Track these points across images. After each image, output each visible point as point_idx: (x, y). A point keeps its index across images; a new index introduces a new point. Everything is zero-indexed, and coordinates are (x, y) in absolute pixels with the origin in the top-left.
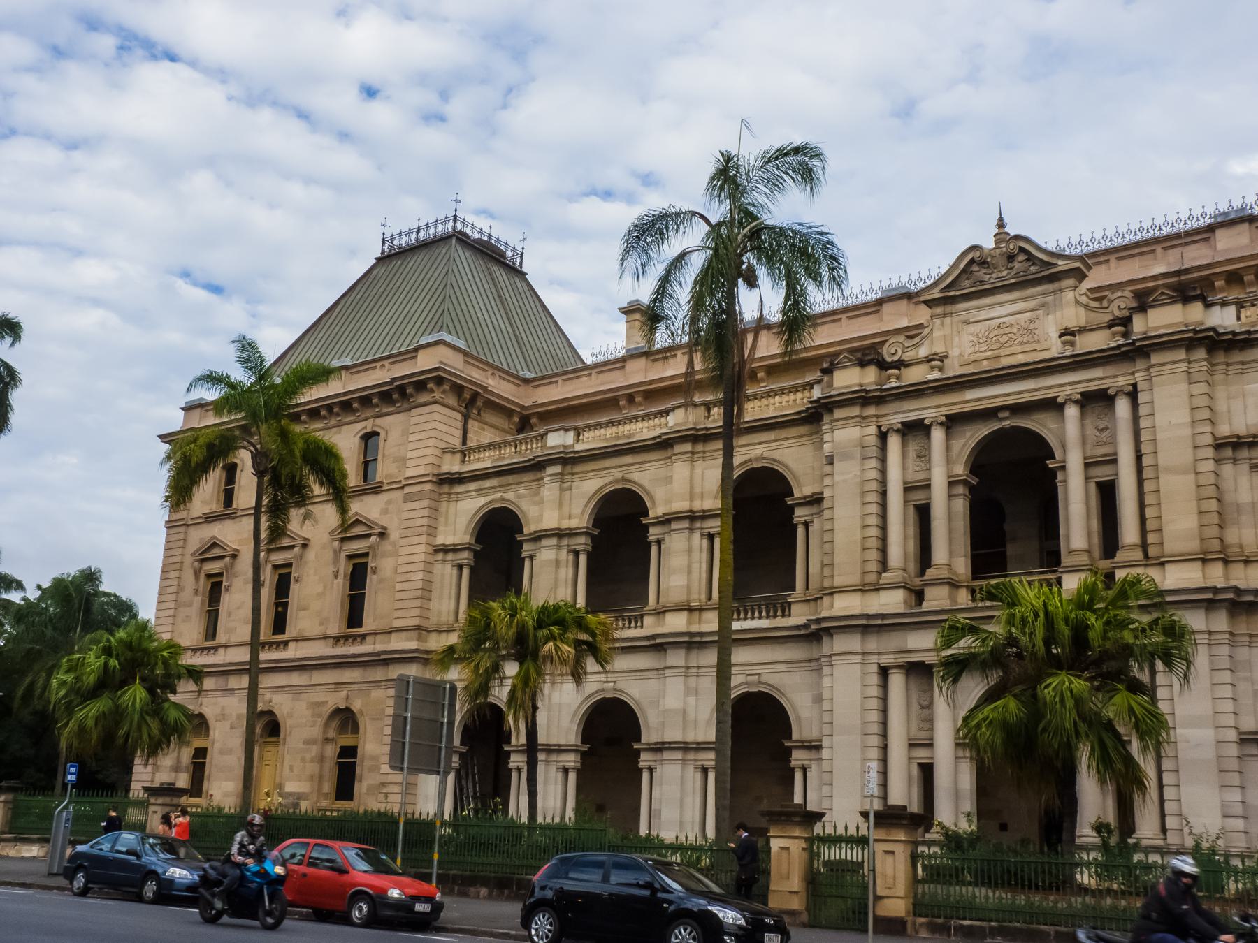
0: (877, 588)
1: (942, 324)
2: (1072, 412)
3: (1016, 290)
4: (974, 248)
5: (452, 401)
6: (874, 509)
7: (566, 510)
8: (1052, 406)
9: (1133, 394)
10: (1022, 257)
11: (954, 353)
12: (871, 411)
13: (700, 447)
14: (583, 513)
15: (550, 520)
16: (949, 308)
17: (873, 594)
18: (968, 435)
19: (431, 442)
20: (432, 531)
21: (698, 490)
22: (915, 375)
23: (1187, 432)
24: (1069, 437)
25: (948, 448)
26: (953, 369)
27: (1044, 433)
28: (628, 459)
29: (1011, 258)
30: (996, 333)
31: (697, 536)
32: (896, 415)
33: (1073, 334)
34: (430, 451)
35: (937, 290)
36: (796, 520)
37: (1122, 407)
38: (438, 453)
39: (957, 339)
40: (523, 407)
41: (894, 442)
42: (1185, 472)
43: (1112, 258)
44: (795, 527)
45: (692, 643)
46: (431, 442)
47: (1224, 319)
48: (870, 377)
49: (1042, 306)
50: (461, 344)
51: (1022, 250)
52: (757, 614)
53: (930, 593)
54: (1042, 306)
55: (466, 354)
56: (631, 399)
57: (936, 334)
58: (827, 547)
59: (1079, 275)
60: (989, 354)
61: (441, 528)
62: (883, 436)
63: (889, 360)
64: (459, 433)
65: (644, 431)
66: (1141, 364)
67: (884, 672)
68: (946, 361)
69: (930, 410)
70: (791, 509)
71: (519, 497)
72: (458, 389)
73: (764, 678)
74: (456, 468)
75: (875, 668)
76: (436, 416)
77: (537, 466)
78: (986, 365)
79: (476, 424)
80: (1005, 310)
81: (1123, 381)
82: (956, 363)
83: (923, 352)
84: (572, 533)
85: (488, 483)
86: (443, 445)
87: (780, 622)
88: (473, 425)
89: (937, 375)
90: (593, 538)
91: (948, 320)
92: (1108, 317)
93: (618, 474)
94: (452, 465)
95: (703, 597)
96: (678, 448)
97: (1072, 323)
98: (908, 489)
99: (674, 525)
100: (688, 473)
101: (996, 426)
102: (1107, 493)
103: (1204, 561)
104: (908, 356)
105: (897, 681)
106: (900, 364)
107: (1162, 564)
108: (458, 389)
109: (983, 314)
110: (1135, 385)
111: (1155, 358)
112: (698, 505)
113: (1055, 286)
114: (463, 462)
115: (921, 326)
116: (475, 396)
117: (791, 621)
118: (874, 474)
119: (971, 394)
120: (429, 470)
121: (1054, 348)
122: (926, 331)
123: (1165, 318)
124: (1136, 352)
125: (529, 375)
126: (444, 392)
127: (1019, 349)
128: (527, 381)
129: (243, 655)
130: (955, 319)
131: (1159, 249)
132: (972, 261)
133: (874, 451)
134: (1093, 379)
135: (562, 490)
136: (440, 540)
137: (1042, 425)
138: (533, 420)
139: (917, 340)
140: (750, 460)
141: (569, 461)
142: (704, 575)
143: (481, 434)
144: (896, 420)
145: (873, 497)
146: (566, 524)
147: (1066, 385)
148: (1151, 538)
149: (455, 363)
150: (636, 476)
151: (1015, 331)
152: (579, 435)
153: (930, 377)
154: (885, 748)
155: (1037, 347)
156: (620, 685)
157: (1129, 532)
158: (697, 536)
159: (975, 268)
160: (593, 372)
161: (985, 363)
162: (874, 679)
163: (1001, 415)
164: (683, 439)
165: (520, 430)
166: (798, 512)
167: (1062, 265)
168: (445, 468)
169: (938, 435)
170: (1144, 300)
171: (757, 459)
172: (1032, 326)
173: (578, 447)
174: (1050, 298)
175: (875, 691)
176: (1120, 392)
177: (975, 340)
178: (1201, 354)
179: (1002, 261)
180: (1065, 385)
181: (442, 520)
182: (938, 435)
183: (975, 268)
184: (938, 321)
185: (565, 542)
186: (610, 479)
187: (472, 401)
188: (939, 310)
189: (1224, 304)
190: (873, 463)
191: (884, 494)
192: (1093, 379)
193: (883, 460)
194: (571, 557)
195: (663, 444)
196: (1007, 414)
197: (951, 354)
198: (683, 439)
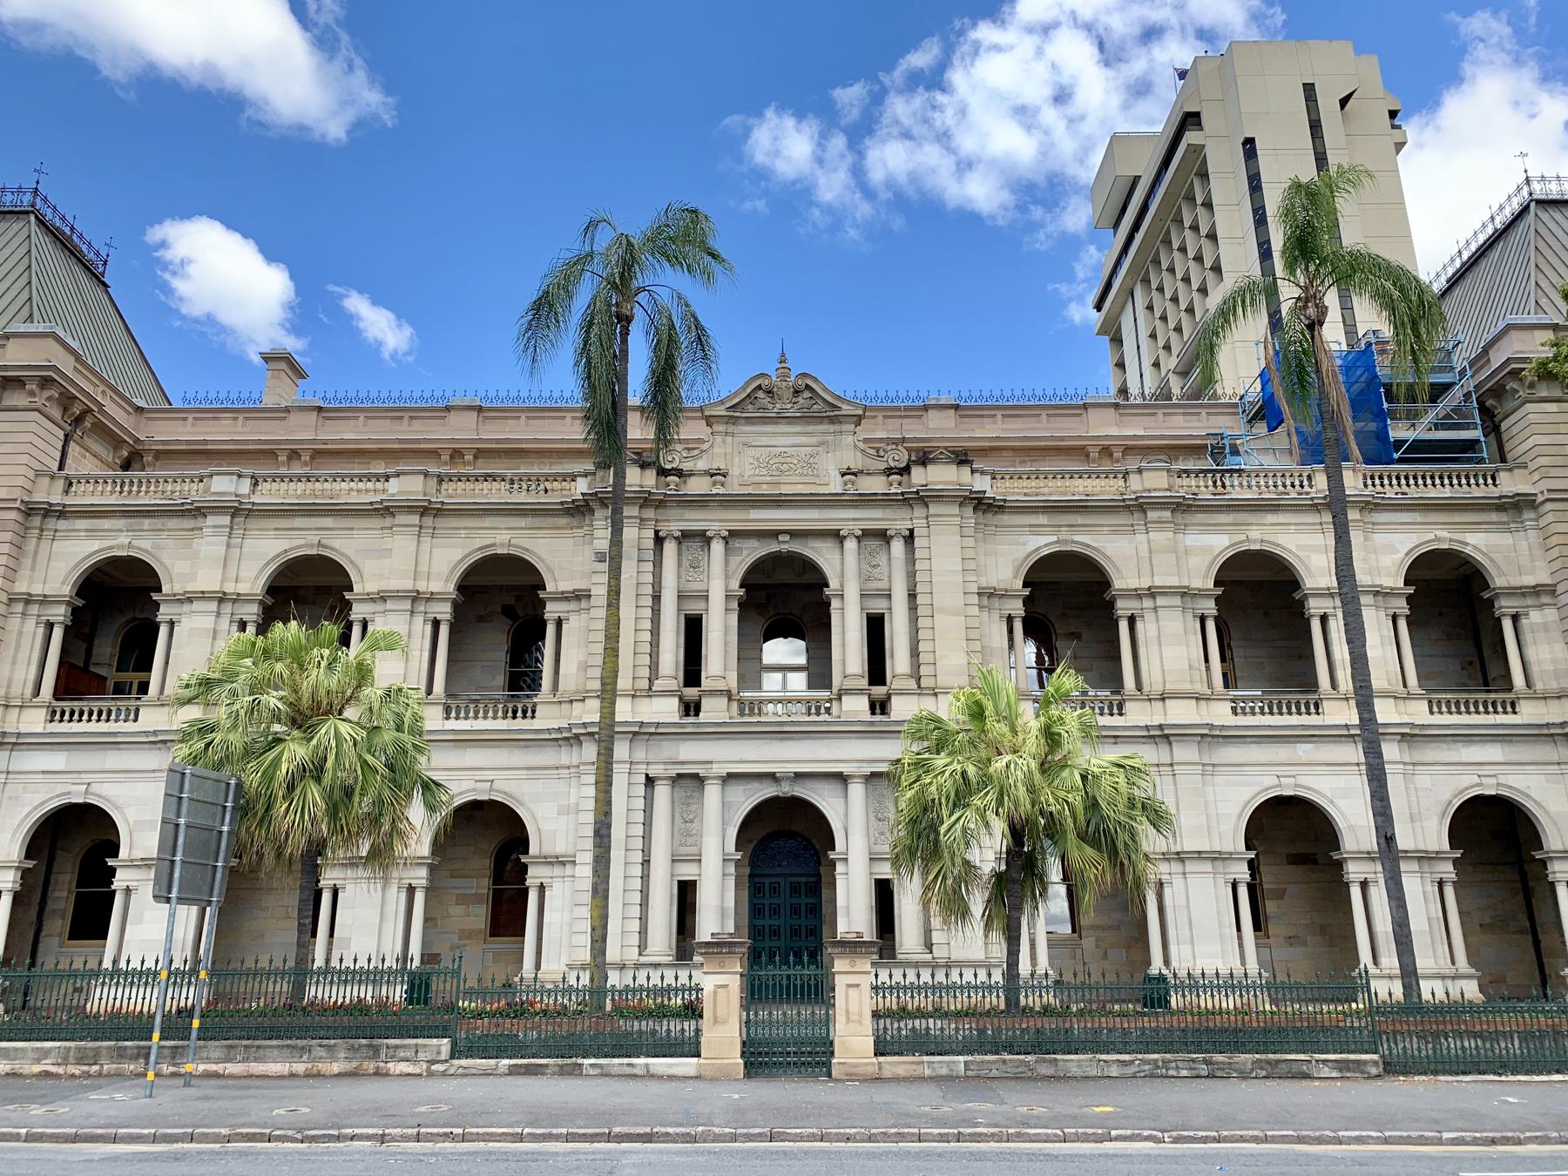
0: (650, 693)
2: (851, 545)
4: (762, 375)
5: (56, 413)
6: (648, 613)
7: (232, 572)
8: (837, 536)
9: (910, 538)
10: (807, 394)
11: (734, 472)
12: (650, 513)
13: (428, 521)
14: (257, 578)
15: (208, 581)
16: (731, 428)
17: (647, 700)
18: (745, 553)
19: (25, 459)
20: (12, 572)
21: (423, 568)
22: (697, 486)
23: (960, 578)
24: (843, 571)
25: (727, 562)
26: (734, 488)
27: (820, 561)
28: (328, 522)
29: (797, 392)
31: (419, 619)
32: (678, 521)
33: (855, 474)
34: (22, 470)
36: (547, 616)
37: (898, 547)
38: (31, 475)
39: (736, 459)
40: (137, 440)
41: (670, 548)
42: (958, 614)
43: (999, 413)
44: (544, 624)
45: (572, 739)
46: (25, 459)
47: (982, 484)
48: (650, 479)
50: (74, 345)
51: (807, 387)
52: (490, 714)
53: (706, 703)
55: (78, 358)
56: (294, 455)
58: (977, 646)
59: (858, 420)
61: (25, 572)
62: (659, 540)
63: (668, 467)
64: (58, 455)
65: (1104, 488)
66: (919, 512)
67: (650, 781)
68: (729, 478)
69: (715, 522)
70: (542, 604)
71: (158, 547)
72: (66, 401)
73: (497, 785)
74: (56, 498)
75: (642, 779)
76: (33, 427)
77: (199, 512)
78: (765, 489)
79: (78, 448)
80: (786, 441)
81: (903, 526)
82: (736, 482)
83: (701, 465)
84: (238, 599)
85: (106, 523)
86: (38, 466)
87: (519, 723)
88: (74, 449)
89: (721, 491)
90: (76, 612)
91: (729, 439)
92: (883, 466)
93: (313, 538)
94: (50, 493)
95: (29, 691)
96: (401, 519)
97: (854, 467)
98: (681, 597)
99: (390, 605)
100: (413, 548)
101: (773, 547)
102: (875, 627)
103: (633, 696)
104: (686, 466)
105: (662, 792)
106: (679, 473)
107: (936, 695)
108: (66, 401)
109: (765, 441)
110: (911, 531)
111: (933, 509)
112: (422, 586)
113: (837, 427)
114: (67, 492)
115: (702, 441)
116: (88, 411)
117: (536, 724)
118: (649, 578)
119: (755, 514)
120: (17, 493)
121: (835, 485)
122: (705, 446)
123: (941, 476)
124: (921, 499)
125: (141, 403)
126: (49, 399)
127: (798, 479)
128: (139, 410)
129: (590, 712)
130: (736, 439)
131: (1044, 413)
132: (759, 387)
133: (650, 555)
134: (874, 518)
135: (228, 546)
136: (21, 587)
137: (823, 555)
138: (148, 458)
139: (695, 452)
140: (493, 545)
141: (239, 512)
142: (425, 665)
143: (81, 463)
144: (675, 527)
145: (649, 601)
146: (230, 588)
147: (850, 520)
148: (924, 670)
149: (66, 365)
150: (336, 543)
152: (256, 484)
154: (646, 862)
156: (1302, 780)
157: (898, 661)
158: (419, 620)
159: (761, 394)
160: (241, 417)
162: (641, 790)
163: (781, 538)
164: (410, 509)
165: (126, 466)
166: (549, 607)
167: (846, 409)
168: (39, 497)
169: (717, 547)
170: (924, 459)
171: (502, 545)
173: (256, 499)
175: (640, 803)
176: (898, 534)
178: (969, 511)
179: (789, 394)
181: (27, 561)
182: (717, 547)
183: (761, 394)
184: (719, 439)
185: (227, 608)
186: (302, 542)
187: (78, 418)
188: (721, 428)
189: (983, 473)
190: (649, 567)
191: (657, 598)
192: (874, 518)
193: (658, 563)
194: (429, 628)
195: (385, 510)
196: (787, 538)
198: (410, 509)
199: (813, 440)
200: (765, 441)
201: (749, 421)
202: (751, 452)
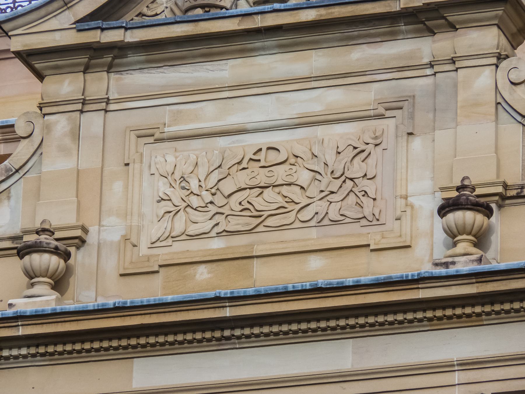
1: (76, 134)
3: (314, 45)
11: (107, 232)
16: (99, 84)
30: (243, 179)
35: (67, 18)
39: (118, 187)
49: (393, 106)
54: (393, 106)
57: (55, 163)
60: (216, 245)
68: (78, 258)
78: (204, 281)
82: (111, 265)
89: (46, 300)
91: (93, 122)
97: (484, 176)
121: (424, 246)
122: (21, 151)
127: (313, 237)
130: (118, 121)
151: (304, 177)
153: (24, 305)
155: (374, 237)
161: (202, 273)
172: (357, 169)
174: (421, 84)
177: (177, 195)
180: (446, 367)
184: (61, 124)
188: (66, 86)
197: (92, 238)
199: (365, 97)
200: (210, 115)
201: (157, 52)
202: (166, 157)
